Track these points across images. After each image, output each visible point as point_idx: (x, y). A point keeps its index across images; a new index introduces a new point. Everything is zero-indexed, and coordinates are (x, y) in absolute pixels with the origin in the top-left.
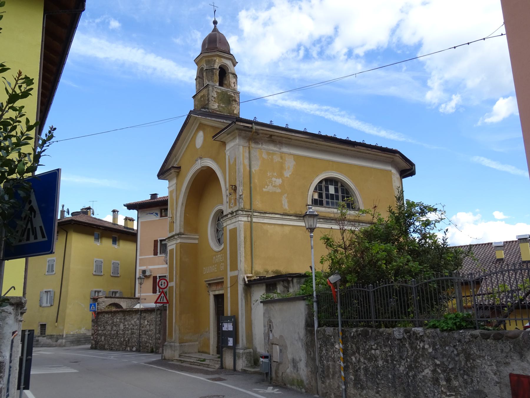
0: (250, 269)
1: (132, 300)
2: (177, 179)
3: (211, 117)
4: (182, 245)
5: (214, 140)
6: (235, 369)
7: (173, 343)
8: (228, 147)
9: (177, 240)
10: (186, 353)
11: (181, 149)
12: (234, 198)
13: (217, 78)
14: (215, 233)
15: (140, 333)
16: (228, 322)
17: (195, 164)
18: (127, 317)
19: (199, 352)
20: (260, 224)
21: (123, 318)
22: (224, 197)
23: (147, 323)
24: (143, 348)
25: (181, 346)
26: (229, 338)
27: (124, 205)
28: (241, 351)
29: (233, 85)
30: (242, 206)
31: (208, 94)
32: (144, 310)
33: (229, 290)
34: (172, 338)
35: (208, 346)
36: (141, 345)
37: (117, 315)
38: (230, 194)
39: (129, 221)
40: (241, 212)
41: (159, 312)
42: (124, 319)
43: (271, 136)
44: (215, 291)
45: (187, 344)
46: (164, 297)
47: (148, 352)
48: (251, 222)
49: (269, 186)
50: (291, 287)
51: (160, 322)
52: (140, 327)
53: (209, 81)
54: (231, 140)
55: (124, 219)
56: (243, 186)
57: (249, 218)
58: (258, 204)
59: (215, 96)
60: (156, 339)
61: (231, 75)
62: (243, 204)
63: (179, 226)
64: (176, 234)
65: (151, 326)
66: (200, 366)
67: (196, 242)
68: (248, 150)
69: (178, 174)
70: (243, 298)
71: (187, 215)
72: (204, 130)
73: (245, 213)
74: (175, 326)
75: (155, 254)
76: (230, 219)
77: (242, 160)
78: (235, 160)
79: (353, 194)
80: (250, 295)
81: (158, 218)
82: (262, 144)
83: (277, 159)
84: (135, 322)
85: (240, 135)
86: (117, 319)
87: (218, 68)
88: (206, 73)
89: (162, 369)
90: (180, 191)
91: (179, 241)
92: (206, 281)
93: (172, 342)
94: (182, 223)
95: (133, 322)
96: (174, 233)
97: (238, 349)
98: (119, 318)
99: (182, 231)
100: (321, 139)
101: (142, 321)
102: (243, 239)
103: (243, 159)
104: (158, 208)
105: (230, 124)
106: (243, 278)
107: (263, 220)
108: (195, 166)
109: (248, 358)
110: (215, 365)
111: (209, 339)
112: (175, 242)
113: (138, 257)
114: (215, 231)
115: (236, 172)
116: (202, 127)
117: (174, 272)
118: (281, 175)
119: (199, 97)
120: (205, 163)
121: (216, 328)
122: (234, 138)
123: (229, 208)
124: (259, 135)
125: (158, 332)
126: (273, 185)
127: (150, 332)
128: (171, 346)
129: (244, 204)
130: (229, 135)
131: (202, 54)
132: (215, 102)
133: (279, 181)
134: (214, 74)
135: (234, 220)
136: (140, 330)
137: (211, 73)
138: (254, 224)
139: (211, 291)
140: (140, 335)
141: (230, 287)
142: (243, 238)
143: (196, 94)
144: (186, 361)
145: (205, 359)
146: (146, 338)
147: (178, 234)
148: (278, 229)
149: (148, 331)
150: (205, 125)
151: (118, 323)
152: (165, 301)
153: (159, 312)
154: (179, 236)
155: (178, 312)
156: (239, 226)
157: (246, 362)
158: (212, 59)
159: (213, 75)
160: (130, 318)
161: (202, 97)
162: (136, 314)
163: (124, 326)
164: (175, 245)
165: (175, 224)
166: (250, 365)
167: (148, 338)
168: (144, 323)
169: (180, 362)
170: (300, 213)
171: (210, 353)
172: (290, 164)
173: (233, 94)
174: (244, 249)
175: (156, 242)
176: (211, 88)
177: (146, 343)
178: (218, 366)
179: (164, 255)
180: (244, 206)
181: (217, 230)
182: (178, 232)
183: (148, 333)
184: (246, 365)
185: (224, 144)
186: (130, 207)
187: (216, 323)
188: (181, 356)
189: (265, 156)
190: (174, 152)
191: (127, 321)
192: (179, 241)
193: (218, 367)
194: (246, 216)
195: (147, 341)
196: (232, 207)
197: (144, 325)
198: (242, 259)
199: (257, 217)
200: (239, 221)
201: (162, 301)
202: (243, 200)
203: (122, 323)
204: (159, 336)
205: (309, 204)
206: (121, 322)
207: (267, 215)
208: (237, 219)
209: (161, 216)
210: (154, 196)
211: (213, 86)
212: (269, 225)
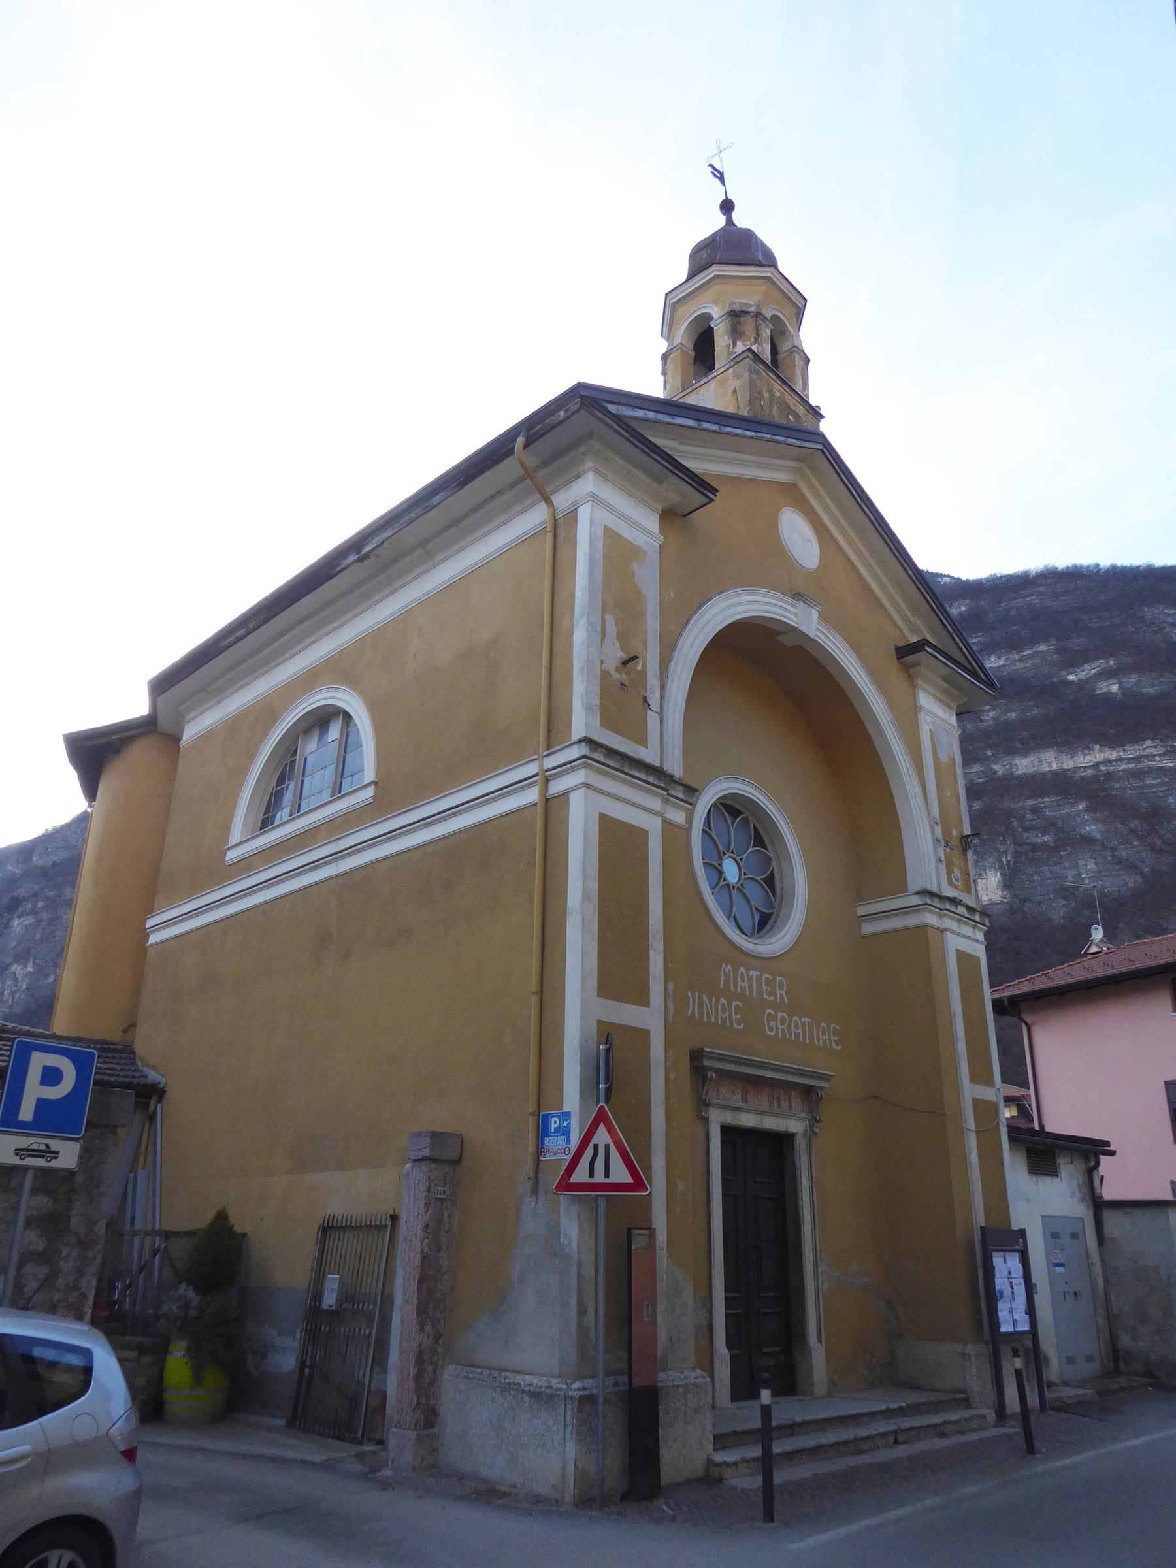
76: (959, 921)
130: (945, 685)
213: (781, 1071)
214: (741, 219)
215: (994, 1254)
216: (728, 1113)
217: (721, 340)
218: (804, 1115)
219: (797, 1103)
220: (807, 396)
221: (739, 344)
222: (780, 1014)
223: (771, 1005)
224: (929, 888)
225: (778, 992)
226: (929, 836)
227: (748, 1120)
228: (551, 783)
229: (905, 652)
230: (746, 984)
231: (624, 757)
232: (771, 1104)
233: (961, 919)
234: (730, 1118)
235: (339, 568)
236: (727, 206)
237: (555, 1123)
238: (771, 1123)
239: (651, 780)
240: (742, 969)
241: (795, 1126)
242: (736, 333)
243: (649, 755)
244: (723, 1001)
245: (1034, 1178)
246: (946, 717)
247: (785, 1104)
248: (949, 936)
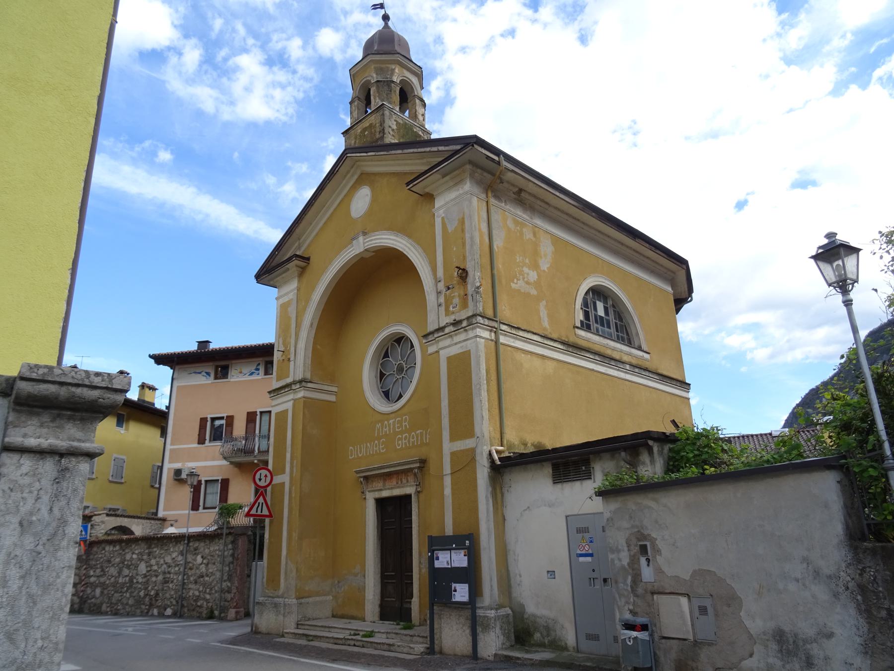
0: (498, 436)
1: (152, 522)
2: (299, 281)
3: (402, 149)
4: (308, 403)
5: (409, 189)
6: (474, 655)
7: (281, 599)
8: (439, 202)
9: (296, 392)
10: (309, 619)
11: (313, 224)
12: (459, 296)
13: (396, 98)
14: (377, 381)
15: (184, 580)
16: (450, 550)
17: (349, 246)
18: (155, 550)
19: (334, 616)
20: (509, 348)
21: (147, 551)
22: (431, 298)
23: (202, 560)
24: (188, 610)
25: (301, 604)
26: (454, 585)
27: (151, 357)
28: (492, 613)
29: (421, 118)
30: (481, 309)
31: (382, 123)
32: (198, 535)
33: (448, 481)
35: (360, 603)
36: (185, 605)
37: (133, 546)
38: (449, 288)
39: (147, 390)
40: (480, 318)
41: (230, 538)
42: (149, 554)
43: (521, 190)
44: (381, 490)
45: (311, 600)
46: (264, 505)
47: (200, 618)
48: (497, 342)
49: (519, 280)
50: (644, 463)
51: (231, 559)
52: (185, 568)
53: (383, 100)
54: (450, 188)
55: (139, 387)
56: (481, 271)
57: (493, 334)
58: (505, 311)
59: (395, 127)
60: (222, 591)
61: (417, 101)
62: (481, 304)
63: (302, 365)
64: (294, 381)
65: (210, 565)
66: (363, 647)
67: (333, 398)
68: (486, 208)
69: (302, 271)
70: (489, 496)
71: (319, 347)
72: (371, 185)
73: (487, 322)
74: (287, 563)
75: (201, 441)
76: (451, 336)
77: (477, 223)
78: (462, 222)
79: (630, 322)
80: (501, 488)
81: (211, 380)
82: (505, 201)
83: (528, 235)
84: (174, 558)
85: (472, 176)
86: (133, 553)
87: (398, 82)
88: (378, 87)
89: (273, 657)
90: (308, 300)
91: (301, 394)
92: (357, 472)
93: (278, 597)
94: (309, 362)
95: (168, 559)
96: (289, 380)
97: (482, 608)
98: (137, 552)
99: (308, 376)
100: (594, 214)
101: (190, 558)
102: (485, 374)
103: (479, 221)
104: (211, 364)
105: (460, 150)
106: (488, 452)
107: (513, 342)
108: (346, 251)
109: (505, 630)
110: (412, 646)
111: (362, 589)
112: (291, 396)
113: (168, 447)
114: (376, 377)
115: (464, 244)
116: (365, 178)
117: (288, 456)
118: (535, 266)
119: (359, 131)
120: (374, 242)
121: (379, 566)
122: (459, 182)
123: (446, 315)
124: (503, 183)
125: (225, 578)
126: (526, 279)
127: (207, 578)
128: (276, 606)
129: (483, 305)
130: (447, 178)
131: (368, 57)
132: (393, 138)
133: (533, 276)
134: (393, 91)
135: (462, 336)
136: (184, 575)
137: (386, 88)
138: (501, 348)
139: (369, 491)
140: (184, 584)
141: (451, 474)
142: (484, 372)
143: (350, 126)
144: (321, 637)
145: (372, 632)
146: (198, 590)
147: (300, 382)
148: (537, 362)
149: (202, 577)
150: (375, 174)
151: (133, 562)
152: (266, 512)
153: (230, 538)
154: (304, 384)
155: (295, 535)
156: (477, 347)
157: (502, 637)
158: (388, 67)
159: (391, 91)
160: (162, 552)
161: (365, 130)
162: (176, 543)
163: (147, 567)
164: (291, 403)
165: (292, 363)
166: (508, 644)
167: (201, 589)
168: (195, 560)
169: (305, 638)
170: (567, 340)
171: (366, 619)
172: (547, 248)
173: (420, 133)
174: (486, 394)
175: (203, 421)
176: (387, 113)
177: (196, 601)
178: (420, 648)
179: (220, 444)
180: (483, 309)
181: (382, 375)
182: (299, 376)
183: (202, 579)
184: (503, 644)
185: (429, 197)
186: (160, 359)
187: (379, 556)
188: (300, 627)
189: (510, 224)
190: (298, 231)
191: (155, 558)
192: (301, 394)
193: (422, 650)
194: (487, 330)
195: (199, 596)
196: (453, 313)
197: (193, 565)
198: (484, 414)
199: (506, 334)
200: (477, 336)
201: (259, 513)
202: (481, 297)
203: (143, 562)
204: (229, 584)
205: (577, 325)
206: (141, 560)
207: (521, 333)
208: (471, 334)
209: (216, 378)
210: (203, 344)
211: (391, 110)
212: (524, 353)
213: (392, 467)
216: (376, 493)
219: (411, 479)
227: (385, 494)
232: (397, 483)
233: (450, 335)
234: (378, 495)
238: (397, 492)
240: (386, 422)
241: (409, 490)
244: (376, 442)
245: (559, 486)
247: (404, 481)
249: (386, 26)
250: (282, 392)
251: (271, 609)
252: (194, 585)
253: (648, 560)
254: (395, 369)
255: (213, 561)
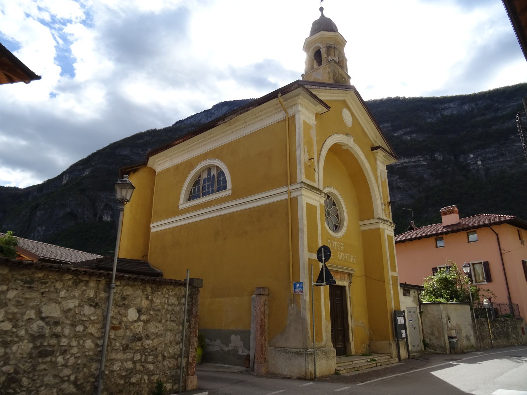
26: (402, 331)
34: (322, 341)
127: (149, 342)
130: (384, 158)
149: (140, 339)
183: (139, 344)
195: (132, 369)
214: (327, 15)
215: (502, 314)
217: (324, 55)
218: (348, 281)
220: (347, 72)
221: (329, 57)
222: (342, 253)
223: (340, 251)
224: (380, 217)
225: (341, 247)
226: (380, 202)
228: (291, 194)
229: (374, 148)
230: (334, 246)
231: (311, 186)
235: (217, 124)
236: (321, 9)
237: (298, 285)
239: (317, 192)
240: (333, 241)
242: (328, 54)
243: (316, 185)
245: (405, 297)
246: (384, 167)
248: (386, 231)
249: (322, 15)
250: (314, 191)
251: (322, 357)
252: (121, 353)
253: (450, 321)
254: (330, 212)
255: (159, 318)
